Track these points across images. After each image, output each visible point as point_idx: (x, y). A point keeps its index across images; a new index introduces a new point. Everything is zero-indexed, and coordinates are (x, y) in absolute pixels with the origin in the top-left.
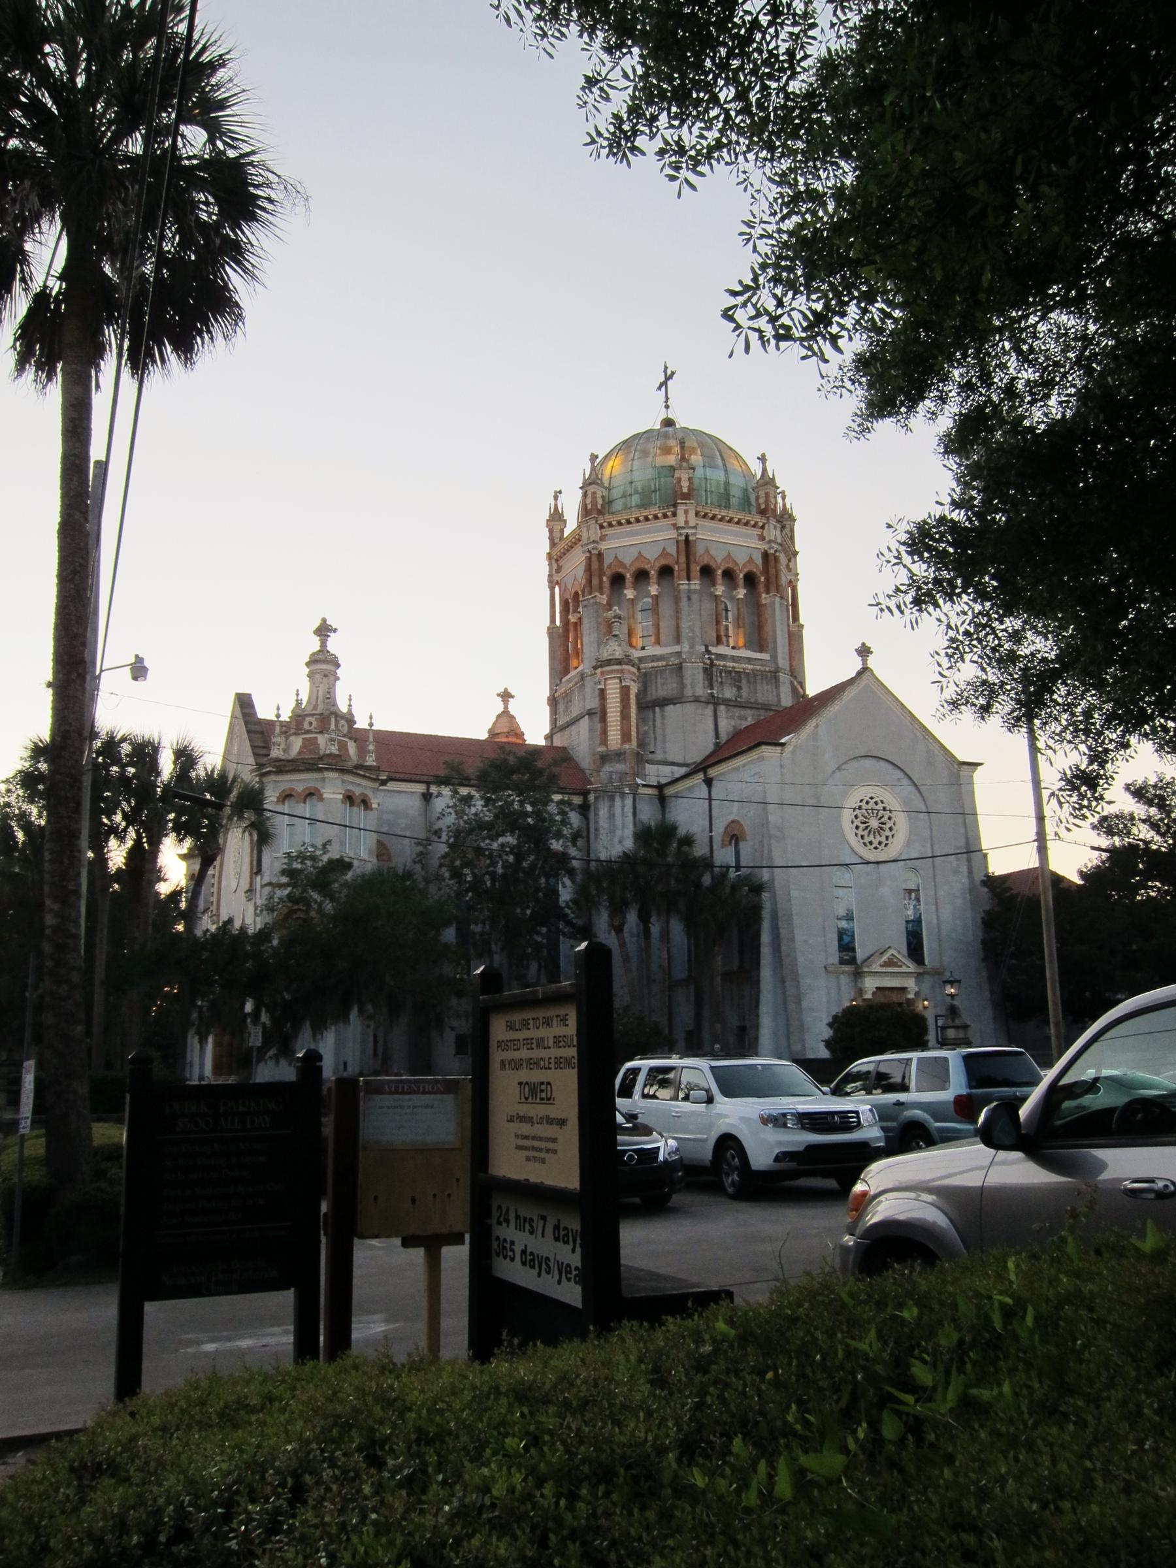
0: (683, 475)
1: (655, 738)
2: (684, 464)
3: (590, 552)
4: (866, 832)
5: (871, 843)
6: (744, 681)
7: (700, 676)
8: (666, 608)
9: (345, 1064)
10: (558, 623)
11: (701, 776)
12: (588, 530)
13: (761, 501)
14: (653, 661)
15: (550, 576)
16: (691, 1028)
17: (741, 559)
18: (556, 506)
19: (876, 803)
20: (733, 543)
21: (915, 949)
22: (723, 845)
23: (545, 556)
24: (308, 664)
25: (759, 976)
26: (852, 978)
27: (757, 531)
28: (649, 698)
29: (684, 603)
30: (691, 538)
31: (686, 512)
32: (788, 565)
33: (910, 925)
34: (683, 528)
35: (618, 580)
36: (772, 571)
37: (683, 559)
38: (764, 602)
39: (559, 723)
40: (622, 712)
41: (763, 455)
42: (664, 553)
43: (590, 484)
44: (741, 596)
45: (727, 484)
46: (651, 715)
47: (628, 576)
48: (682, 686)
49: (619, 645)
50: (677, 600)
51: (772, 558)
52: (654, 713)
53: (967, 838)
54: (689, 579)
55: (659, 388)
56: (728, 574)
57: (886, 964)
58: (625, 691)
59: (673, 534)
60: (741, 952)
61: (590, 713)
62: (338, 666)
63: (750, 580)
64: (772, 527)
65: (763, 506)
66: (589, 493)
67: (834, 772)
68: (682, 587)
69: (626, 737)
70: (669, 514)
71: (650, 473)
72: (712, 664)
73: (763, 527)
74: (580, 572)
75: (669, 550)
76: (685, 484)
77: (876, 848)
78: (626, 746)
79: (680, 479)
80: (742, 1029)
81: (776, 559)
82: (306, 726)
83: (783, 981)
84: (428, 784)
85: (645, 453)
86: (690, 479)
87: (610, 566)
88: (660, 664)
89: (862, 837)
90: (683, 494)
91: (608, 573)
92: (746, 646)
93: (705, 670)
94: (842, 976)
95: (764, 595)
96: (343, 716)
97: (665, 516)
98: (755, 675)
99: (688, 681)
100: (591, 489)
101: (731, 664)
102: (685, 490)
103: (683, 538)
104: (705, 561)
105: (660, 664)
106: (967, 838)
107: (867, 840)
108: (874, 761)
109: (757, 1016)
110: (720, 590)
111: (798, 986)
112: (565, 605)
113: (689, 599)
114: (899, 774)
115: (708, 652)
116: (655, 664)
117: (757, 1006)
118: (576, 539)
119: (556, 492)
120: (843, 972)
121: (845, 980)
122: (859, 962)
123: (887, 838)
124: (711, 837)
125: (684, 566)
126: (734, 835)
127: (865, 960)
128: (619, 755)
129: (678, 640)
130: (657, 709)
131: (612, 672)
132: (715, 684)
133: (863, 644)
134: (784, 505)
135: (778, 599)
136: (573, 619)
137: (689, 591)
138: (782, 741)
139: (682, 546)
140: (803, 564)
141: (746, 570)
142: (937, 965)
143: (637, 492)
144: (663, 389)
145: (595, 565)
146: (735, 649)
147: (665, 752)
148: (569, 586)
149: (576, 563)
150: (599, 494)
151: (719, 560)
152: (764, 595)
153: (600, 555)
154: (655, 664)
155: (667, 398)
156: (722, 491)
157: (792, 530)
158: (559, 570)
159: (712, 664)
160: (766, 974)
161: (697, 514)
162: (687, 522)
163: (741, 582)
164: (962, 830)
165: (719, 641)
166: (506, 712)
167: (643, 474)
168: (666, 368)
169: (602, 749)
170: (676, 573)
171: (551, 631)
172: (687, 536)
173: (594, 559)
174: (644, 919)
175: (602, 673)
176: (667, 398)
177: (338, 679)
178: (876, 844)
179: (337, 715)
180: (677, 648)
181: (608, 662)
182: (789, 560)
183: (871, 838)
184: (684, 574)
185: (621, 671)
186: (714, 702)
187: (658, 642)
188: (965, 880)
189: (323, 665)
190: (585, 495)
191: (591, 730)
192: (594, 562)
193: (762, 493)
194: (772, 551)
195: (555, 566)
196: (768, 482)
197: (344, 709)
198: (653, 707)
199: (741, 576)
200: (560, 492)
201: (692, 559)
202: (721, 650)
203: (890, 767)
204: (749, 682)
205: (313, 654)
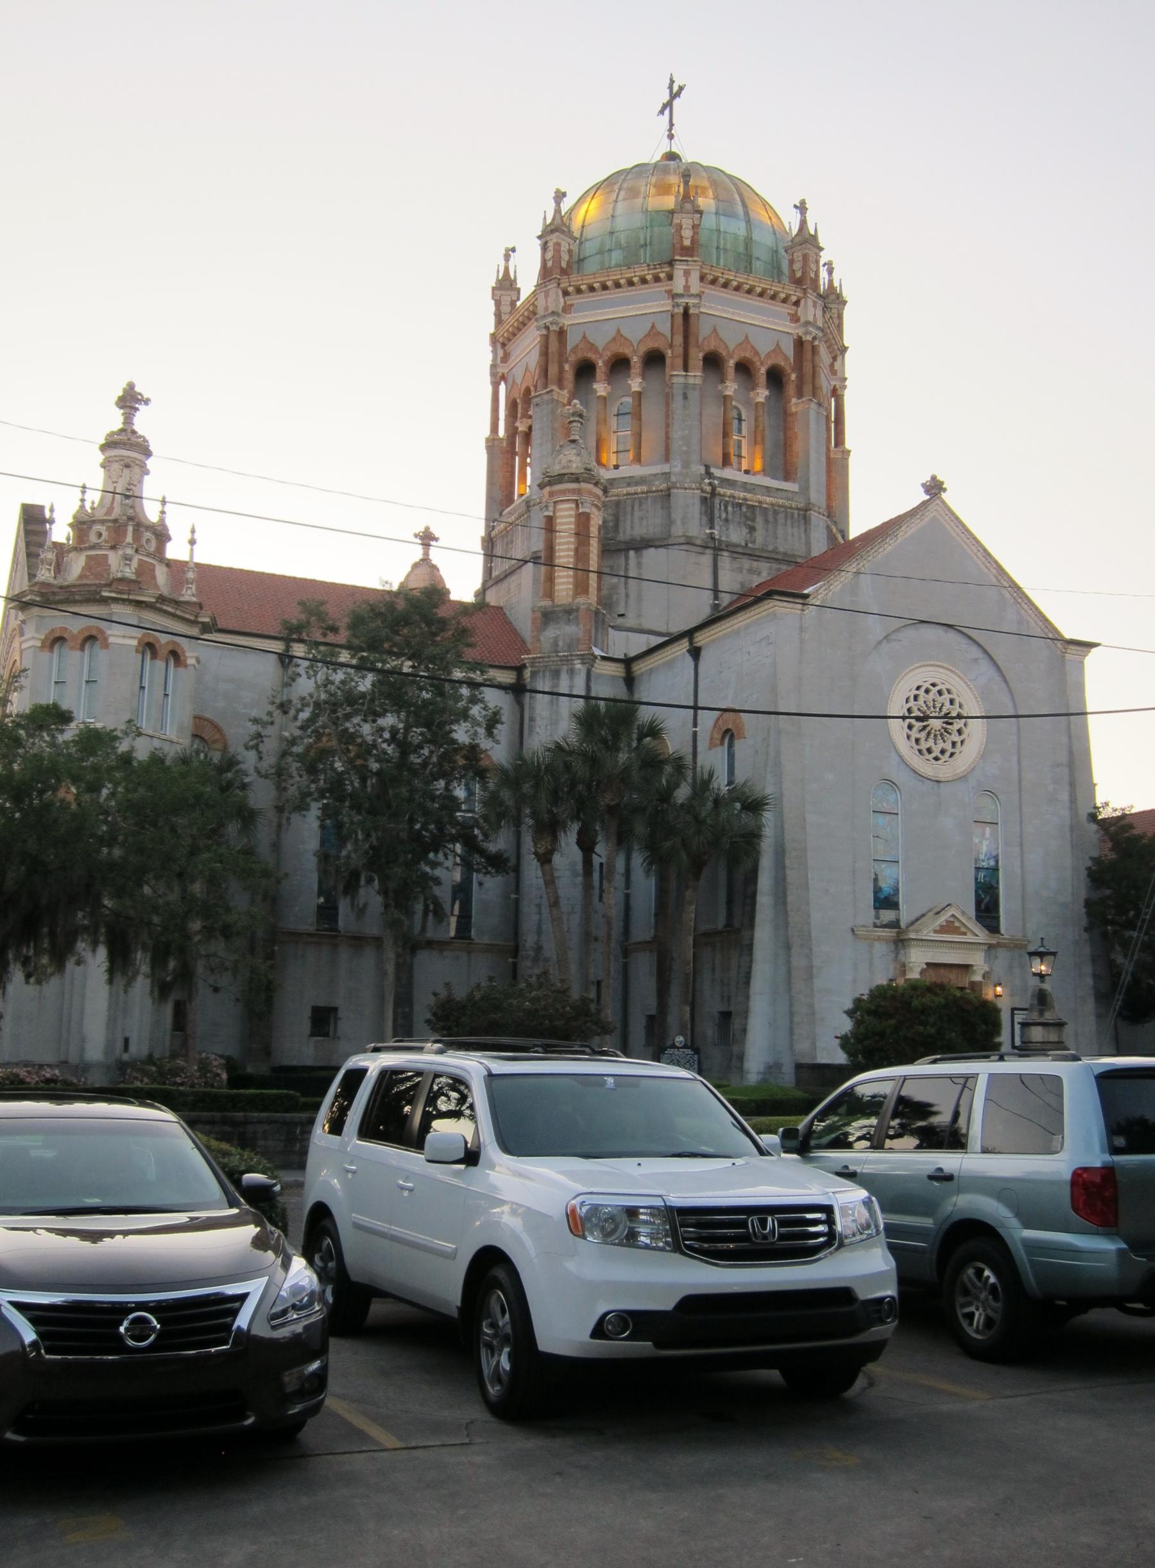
0: (686, 222)
1: (627, 595)
2: (688, 206)
3: (547, 328)
4: (923, 735)
5: (929, 751)
6: (759, 520)
7: (696, 509)
8: (652, 412)
9: (126, 1041)
10: (501, 432)
11: (684, 644)
12: (547, 296)
13: (797, 266)
14: (629, 485)
15: (493, 366)
16: (653, 1012)
17: (764, 346)
18: (507, 269)
19: (940, 693)
20: (756, 326)
21: (987, 909)
22: (712, 745)
23: (487, 340)
24: (103, 448)
25: (752, 939)
26: (893, 948)
27: (791, 310)
28: (621, 537)
29: (677, 403)
30: (691, 311)
31: (687, 273)
32: (832, 366)
33: (982, 875)
34: (681, 296)
35: (585, 370)
36: (807, 367)
37: (679, 340)
38: (794, 409)
39: (495, 573)
40: (576, 550)
41: (803, 202)
42: (653, 332)
43: (552, 231)
44: (761, 399)
45: (749, 241)
46: (622, 561)
47: (600, 363)
48: (670, 522)
49: (578, 455)
50: (668, 399)
51: (808, 348)
52: (627, 558)
53: (1071, 753)
54: (686, 369)
55: (662, 112)
56: (744, 369)
57: (943, 930)
58: (583, 520)
59: (666, 305)
60: (730, 902)
61: (535, 559)
62: (148, 453)
63: (776, 378)
64: (810, 303)
65: (799, 274)
66: (550, 244)
67: (880, 643)
68: (675, 380)
69: (581, 587)
70: (662, 275)
71: (638, 221)
72: (713, 493)
73: (797, 303)
74: (534, 359)
76: (687, 234)
77: (936, 759)
78: (581, 600)
79: (680, 227)
80: (726, 1016)
81: (814, 350)
82: (93, 538)
83: (788, 947)
84: (288, 641)
85: (634, 193)
86: (695, 227)
87: (574, 350)
88: (639, 489)
89: (917, 741)
91: (573, 358)
92: (764, 471)
93: (704, 500)
94: (876, 944)
95: (794, 400)
96: (151, 528)
97: (657, 279)
98: (776, 513)
99: (677, 515)
100: (554, 238)
101: (742, 495)
102: (687, 243)
103: (681, 310)
104: (712, 345)
105: (639, 489)
106: (1071, 753)
107: (924, 746)
108: (940, 631)
109: (748, 997)
110: (731, 387)
111: (809, 956)
112: (512, 406)
113: (685, 397)
114: (975, 652)
115: (709, 474)
116: (632, 490)
117: (747, 983)
118: (531, 313)
119: (507, 250)
120: (879, 939)
121: (881, 950)
122: (903, 925)
123: (954, 744)
124: (695, 734)
125: (680, 350)
126: (728, 730)
127: (913, 923)
128: (570, 612)
129: (667, 458)
130: (632, 553)
131: (564, 492)
132: (717, 521)
133: (934, 478)
134: (831, 282)
135: (813, 406)
136: (522, 427)
137: (686, 386)
138: (806, 592)
139: (679, 320)
140: (853, 365)
141: (770, 363)
142: (1019, 935)
143: (619, 246)
144: (667, 112)
146: (749, 472)
147: (639, 616)
148: (519, 381)
150: (564, 247)
151: (731, 347)
152: (794, 400)
153: (562, 333)
154: (632, 490)
155: (671, 125)
156: (741, 250)
157: (840, 317)
158: (505, 359)
159: (713, 493)
160: (763, 935)
161: (702, 278)
162: (687, 287)
164: (1065, 740)
165: (726, 462)
166: (426, 560)
167: (628, 219)
168: (672, 82)
169: (547, 603)
170: (668, 361)
171: (492, 444)
172: (686, 309)
173: (553, 340)
174: (586, 845)
175: (551, 494)
176: (671, 125)
177: (147, 473)
178: (936, 753)
179: (140, 525)
181: (560, 478)
182: (835, 359)
183: (931, 743)
184: (679, 362)
185: (579, 492)
186: (716, 547)
187: (638, 459)
188: (1066, 813)
189: (126, 450)
190: (544, 248)
191: (536, 581)
192: (555, 340)
193: (798, 256)
194: (809, 338)
195: (500, 353)
196: (807, 242)
197: (151, 513)
198: (627, 550)
199: (763, 370)
200: (513, 250)
201: (692, 340)
202: (729, 473)
204: (767, 521)
205: (112, 434)
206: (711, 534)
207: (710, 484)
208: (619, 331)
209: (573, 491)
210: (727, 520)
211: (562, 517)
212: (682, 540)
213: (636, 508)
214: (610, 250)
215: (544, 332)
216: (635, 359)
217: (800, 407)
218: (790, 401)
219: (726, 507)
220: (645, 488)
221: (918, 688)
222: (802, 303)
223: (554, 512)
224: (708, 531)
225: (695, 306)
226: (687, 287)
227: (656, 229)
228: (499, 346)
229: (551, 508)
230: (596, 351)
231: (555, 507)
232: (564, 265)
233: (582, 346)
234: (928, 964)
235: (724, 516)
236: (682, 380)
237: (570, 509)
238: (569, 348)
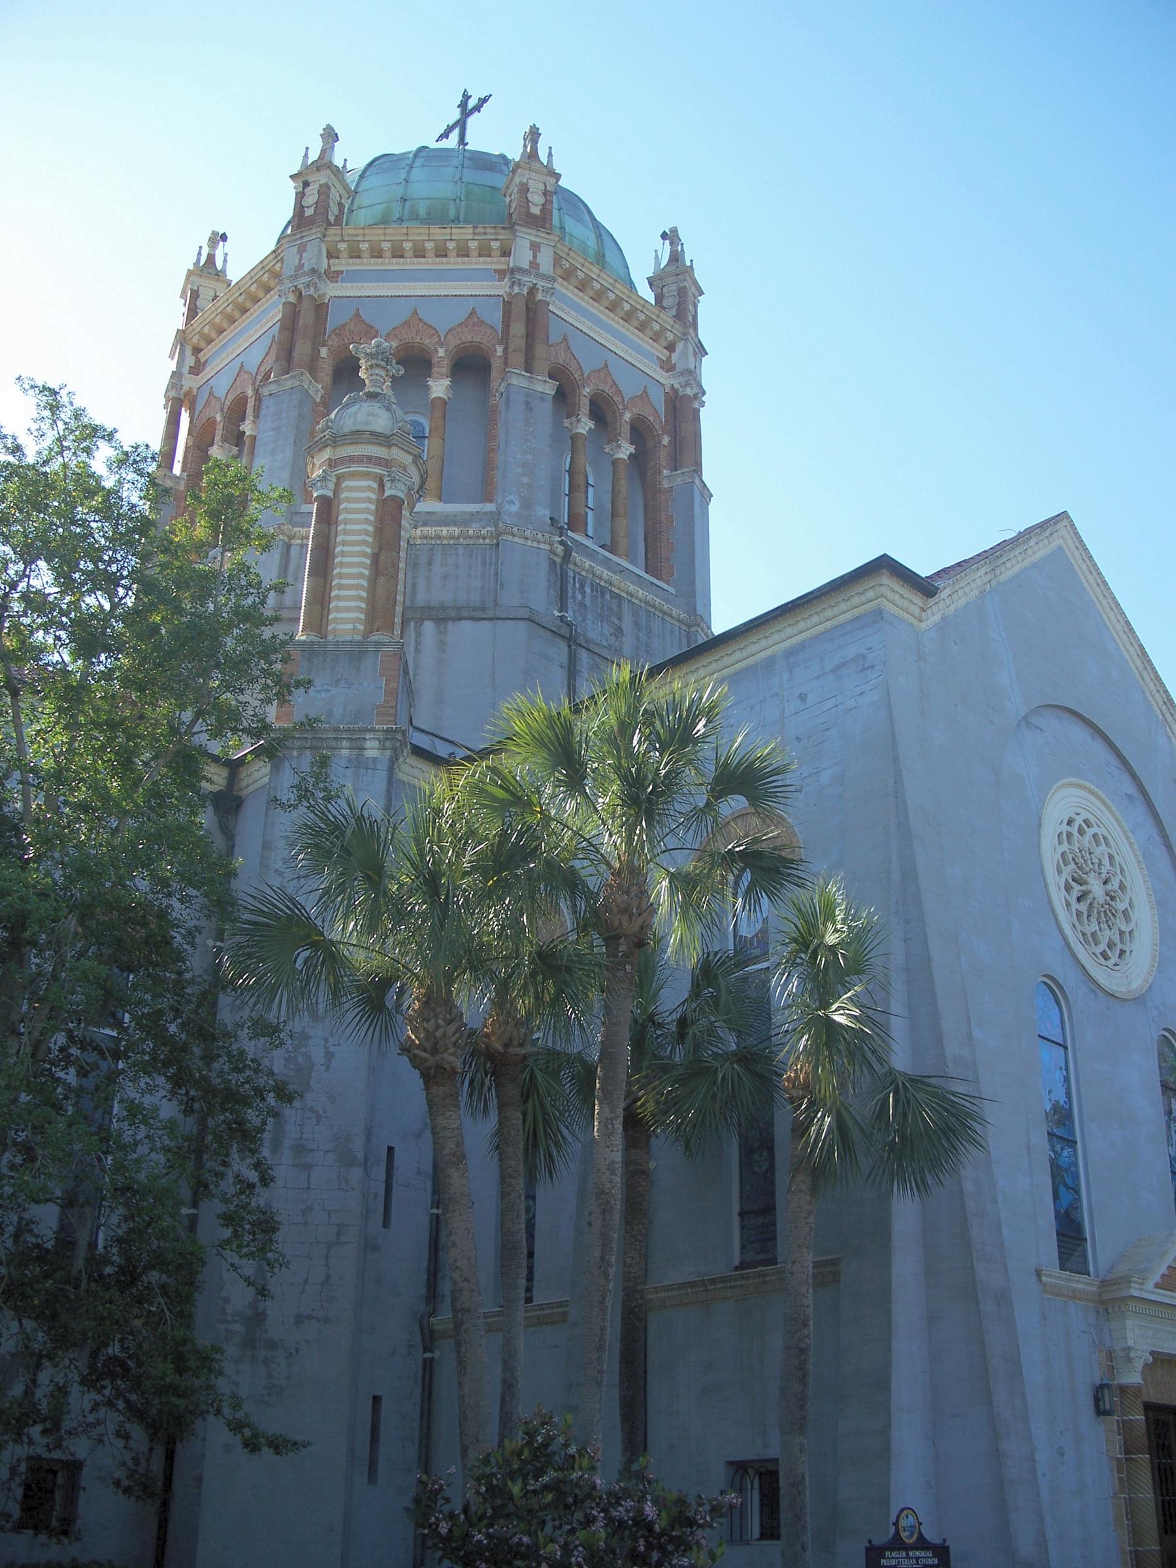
4: (1083, 907)
10: (177, 469)
18: (211, 258)
30: (540, 297)
31: (535, 247)
37: (518, 329)
38: (666, 484)
40: (375, 557)
42: (473, 319)
56: (601, 411)
73: (671, 348)
75: (484, 315)
76: (536, 199)
87: (339, 331)
88: (444, 531)
90: (529, 215)
97: (484, 252)
102: (535, 210)
103: (525, 291)
119: (215, 233)
130: (429, 626)
145: (307, 317)
149: (252, 341)
150: (334, 195)
158: (196, 370)
162: (534, 265)
163: (626, 430)
170: (496, 363)
172: (533, 290)
180: (490, 507)
184: (518, 358)
195: (190, 361)
199: (627, 416)
200: (224, 238)
203: (1114, 761)
206: (562, 618)
207: (562, 543)
208: (415, 313)
209: (378, 461)
210: (582, 605)
211: (348, 500)
212: (524, 613)
213: (437, 560)
216: (441, 352)
217: (679, 480)
218: (660, 472)
219: (582, 586)
220: (456, 531)
221: (1070, 823)
222: (680, 347)
223: (336, 493)
224: (557, 614)
225: (546, 291)
226: (534, 265)
228: (189, 351)
229: (331, 485)
231: (337, 485)
232: (332, 219)
233: (352, 326)
235: (579, 597)
236: (524, 384)
237: (369, 488)
238: (329, 327)
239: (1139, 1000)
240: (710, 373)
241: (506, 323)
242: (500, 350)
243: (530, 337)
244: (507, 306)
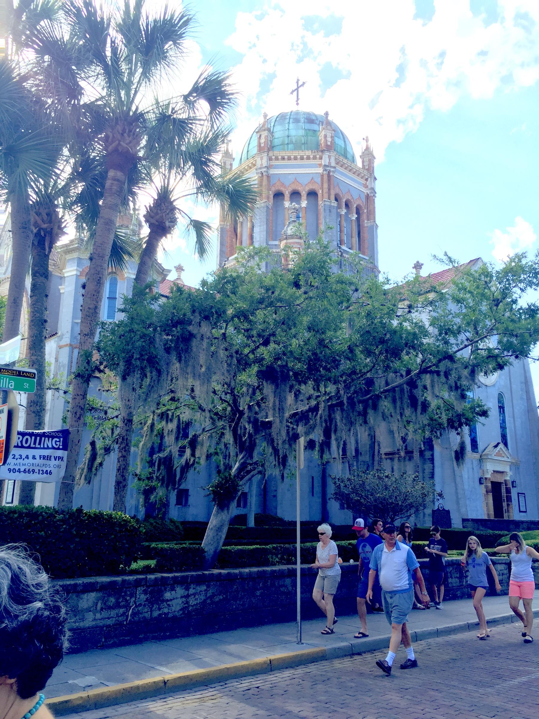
30: (331, 174)
31: (330, 157)
37: (326, 186)
55: (292, 93)
65: (367, 167)
70: (318, 156)
73: (367, 180)
75: (315, 180)
90: (327, 146)
91: (273, 189)
95: (366, 221)
97: (315, 158)
102: (329, 143)
104: (337, 191)
106: (526, 377)
110: (344, 211)
113: (330, 211)
143: (292, 142)
155: (298, 99)
162: (329, 163)
168: (298, 80)
173: (265, 178)
176: (298, 99)
199: (355, 206)
214: (288, 144)
215: (260, 175)
222: (369, 179)
225: (333, 172)
227: (309, 137)
230: (285, 187)
234: (494, 471)
236: (329, 203)
239: (494, 385)
240: (378, 186)
241: (322, 183)
242: (320, 191)
243: (329, 189)
244: (322, 176)
